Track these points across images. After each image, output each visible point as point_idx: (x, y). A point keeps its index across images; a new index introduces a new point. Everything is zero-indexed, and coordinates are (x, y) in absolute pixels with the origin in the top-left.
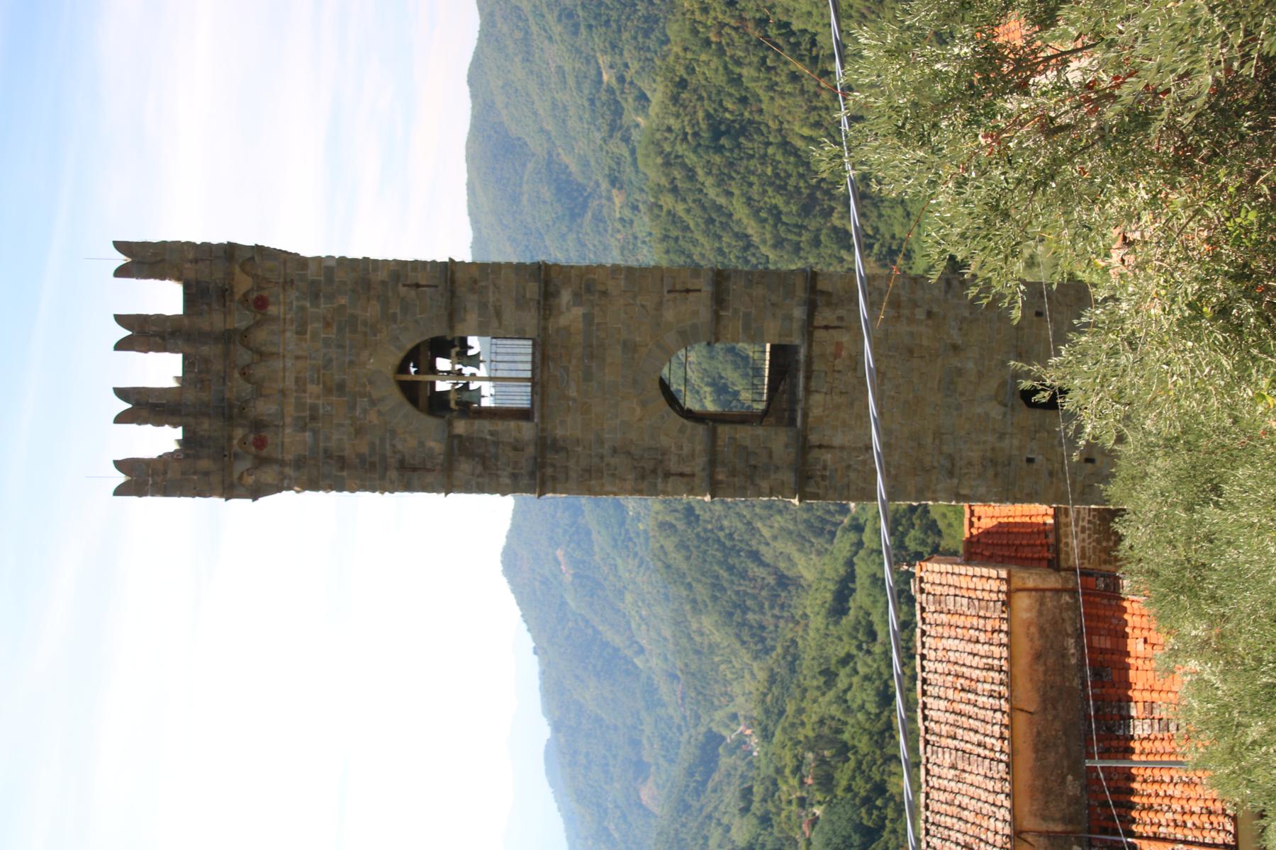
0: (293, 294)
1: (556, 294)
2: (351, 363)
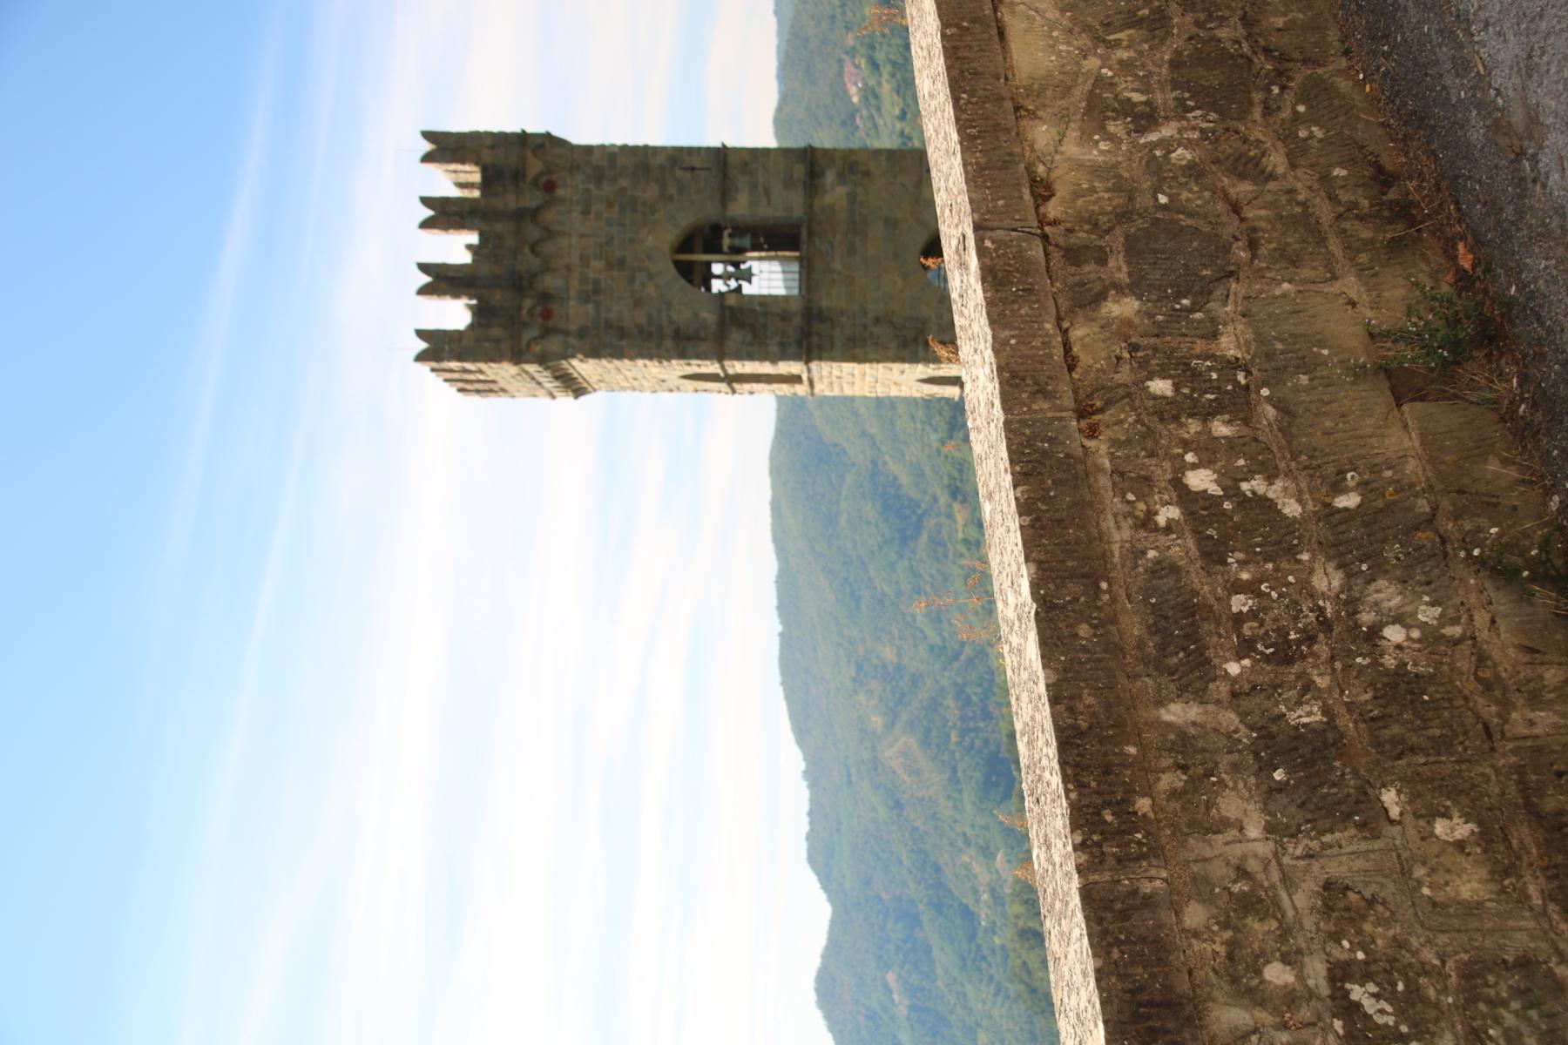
0: (579, 177)
1: (822, 174)
2: (632, 241)
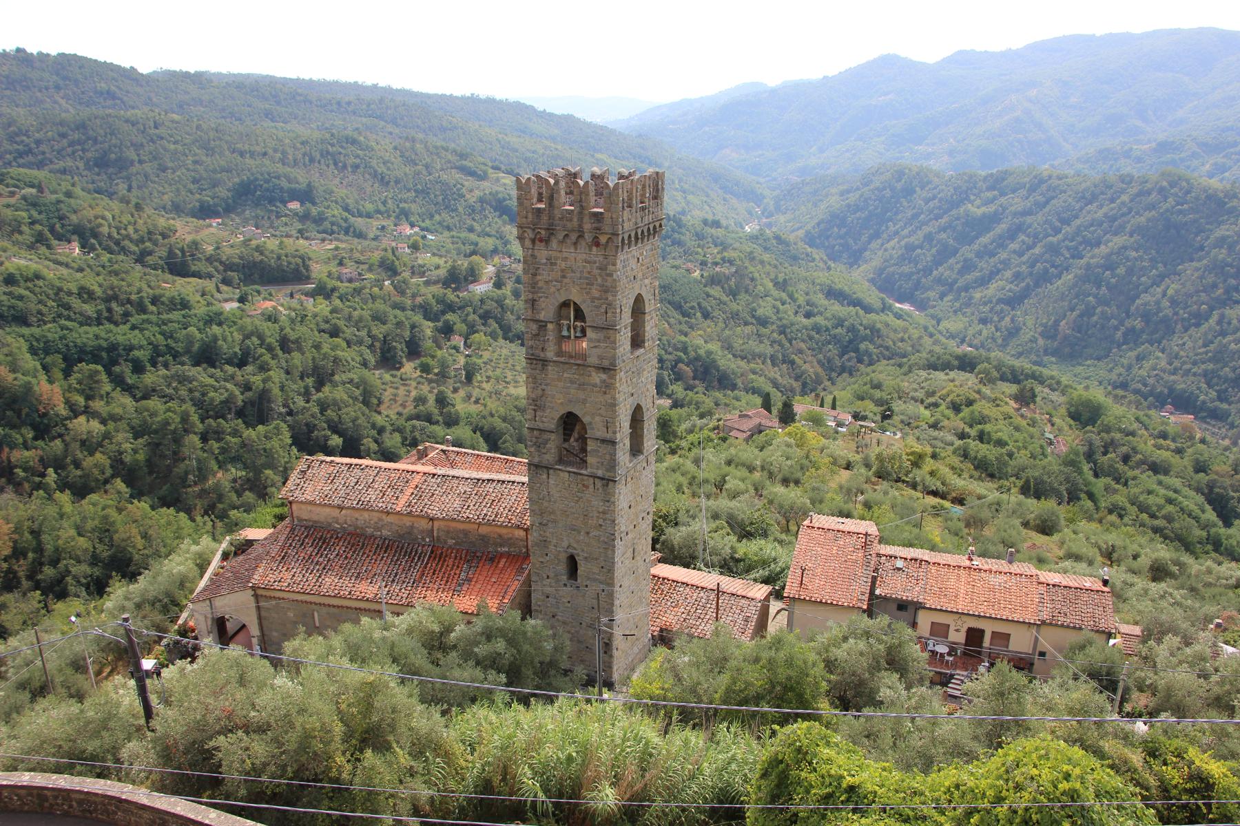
0: (601, 258)
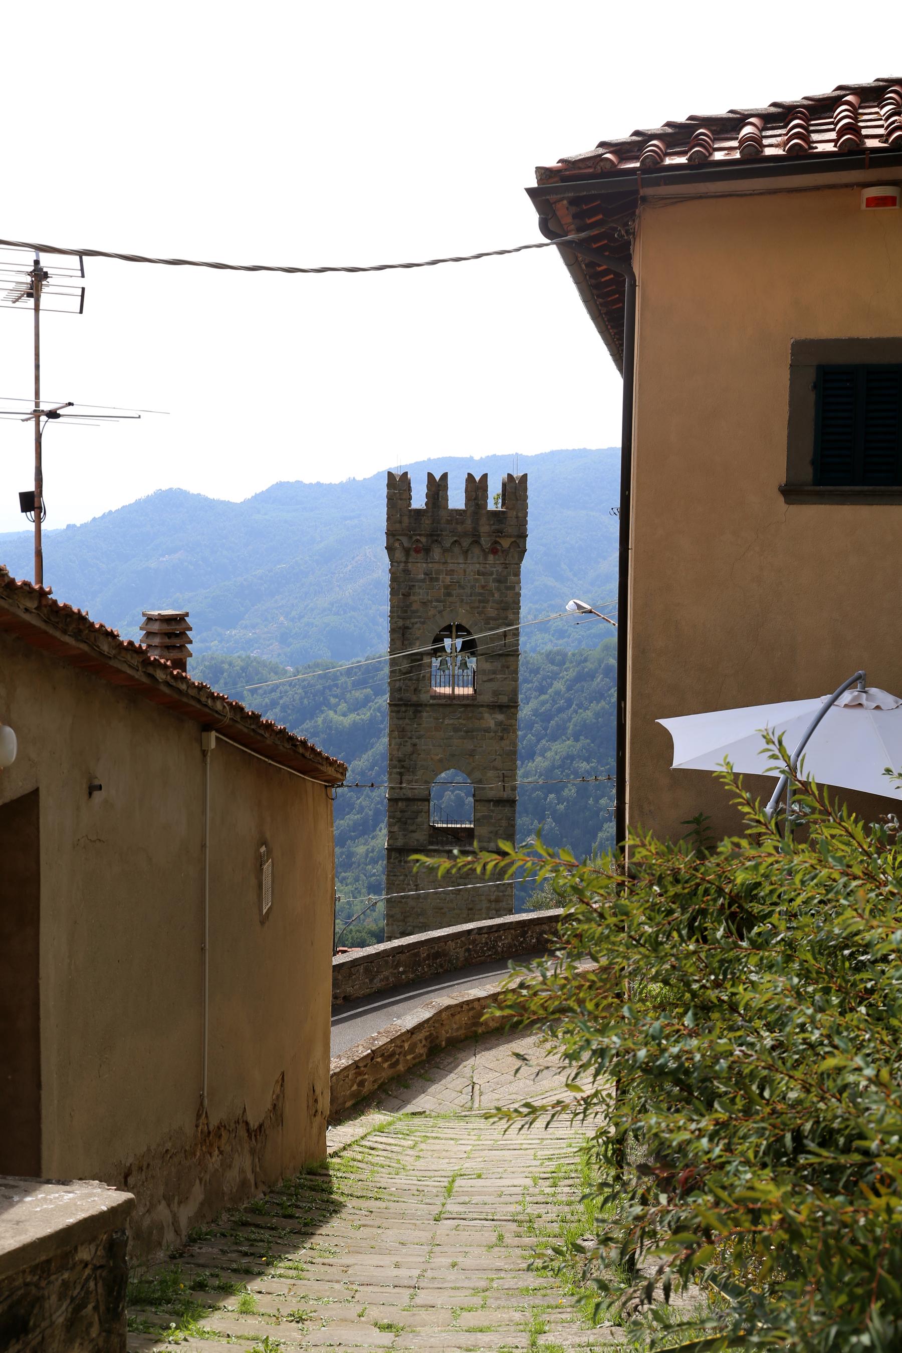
1: (502, 713)
2: (462, 601)
